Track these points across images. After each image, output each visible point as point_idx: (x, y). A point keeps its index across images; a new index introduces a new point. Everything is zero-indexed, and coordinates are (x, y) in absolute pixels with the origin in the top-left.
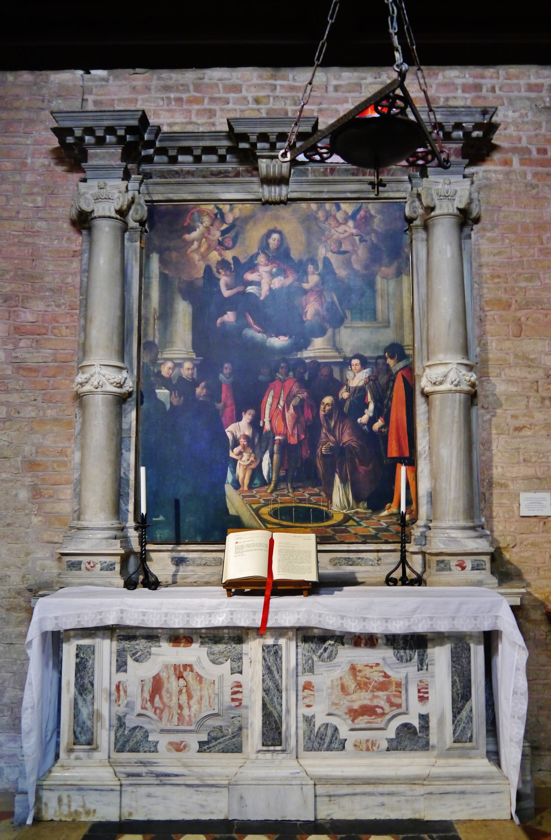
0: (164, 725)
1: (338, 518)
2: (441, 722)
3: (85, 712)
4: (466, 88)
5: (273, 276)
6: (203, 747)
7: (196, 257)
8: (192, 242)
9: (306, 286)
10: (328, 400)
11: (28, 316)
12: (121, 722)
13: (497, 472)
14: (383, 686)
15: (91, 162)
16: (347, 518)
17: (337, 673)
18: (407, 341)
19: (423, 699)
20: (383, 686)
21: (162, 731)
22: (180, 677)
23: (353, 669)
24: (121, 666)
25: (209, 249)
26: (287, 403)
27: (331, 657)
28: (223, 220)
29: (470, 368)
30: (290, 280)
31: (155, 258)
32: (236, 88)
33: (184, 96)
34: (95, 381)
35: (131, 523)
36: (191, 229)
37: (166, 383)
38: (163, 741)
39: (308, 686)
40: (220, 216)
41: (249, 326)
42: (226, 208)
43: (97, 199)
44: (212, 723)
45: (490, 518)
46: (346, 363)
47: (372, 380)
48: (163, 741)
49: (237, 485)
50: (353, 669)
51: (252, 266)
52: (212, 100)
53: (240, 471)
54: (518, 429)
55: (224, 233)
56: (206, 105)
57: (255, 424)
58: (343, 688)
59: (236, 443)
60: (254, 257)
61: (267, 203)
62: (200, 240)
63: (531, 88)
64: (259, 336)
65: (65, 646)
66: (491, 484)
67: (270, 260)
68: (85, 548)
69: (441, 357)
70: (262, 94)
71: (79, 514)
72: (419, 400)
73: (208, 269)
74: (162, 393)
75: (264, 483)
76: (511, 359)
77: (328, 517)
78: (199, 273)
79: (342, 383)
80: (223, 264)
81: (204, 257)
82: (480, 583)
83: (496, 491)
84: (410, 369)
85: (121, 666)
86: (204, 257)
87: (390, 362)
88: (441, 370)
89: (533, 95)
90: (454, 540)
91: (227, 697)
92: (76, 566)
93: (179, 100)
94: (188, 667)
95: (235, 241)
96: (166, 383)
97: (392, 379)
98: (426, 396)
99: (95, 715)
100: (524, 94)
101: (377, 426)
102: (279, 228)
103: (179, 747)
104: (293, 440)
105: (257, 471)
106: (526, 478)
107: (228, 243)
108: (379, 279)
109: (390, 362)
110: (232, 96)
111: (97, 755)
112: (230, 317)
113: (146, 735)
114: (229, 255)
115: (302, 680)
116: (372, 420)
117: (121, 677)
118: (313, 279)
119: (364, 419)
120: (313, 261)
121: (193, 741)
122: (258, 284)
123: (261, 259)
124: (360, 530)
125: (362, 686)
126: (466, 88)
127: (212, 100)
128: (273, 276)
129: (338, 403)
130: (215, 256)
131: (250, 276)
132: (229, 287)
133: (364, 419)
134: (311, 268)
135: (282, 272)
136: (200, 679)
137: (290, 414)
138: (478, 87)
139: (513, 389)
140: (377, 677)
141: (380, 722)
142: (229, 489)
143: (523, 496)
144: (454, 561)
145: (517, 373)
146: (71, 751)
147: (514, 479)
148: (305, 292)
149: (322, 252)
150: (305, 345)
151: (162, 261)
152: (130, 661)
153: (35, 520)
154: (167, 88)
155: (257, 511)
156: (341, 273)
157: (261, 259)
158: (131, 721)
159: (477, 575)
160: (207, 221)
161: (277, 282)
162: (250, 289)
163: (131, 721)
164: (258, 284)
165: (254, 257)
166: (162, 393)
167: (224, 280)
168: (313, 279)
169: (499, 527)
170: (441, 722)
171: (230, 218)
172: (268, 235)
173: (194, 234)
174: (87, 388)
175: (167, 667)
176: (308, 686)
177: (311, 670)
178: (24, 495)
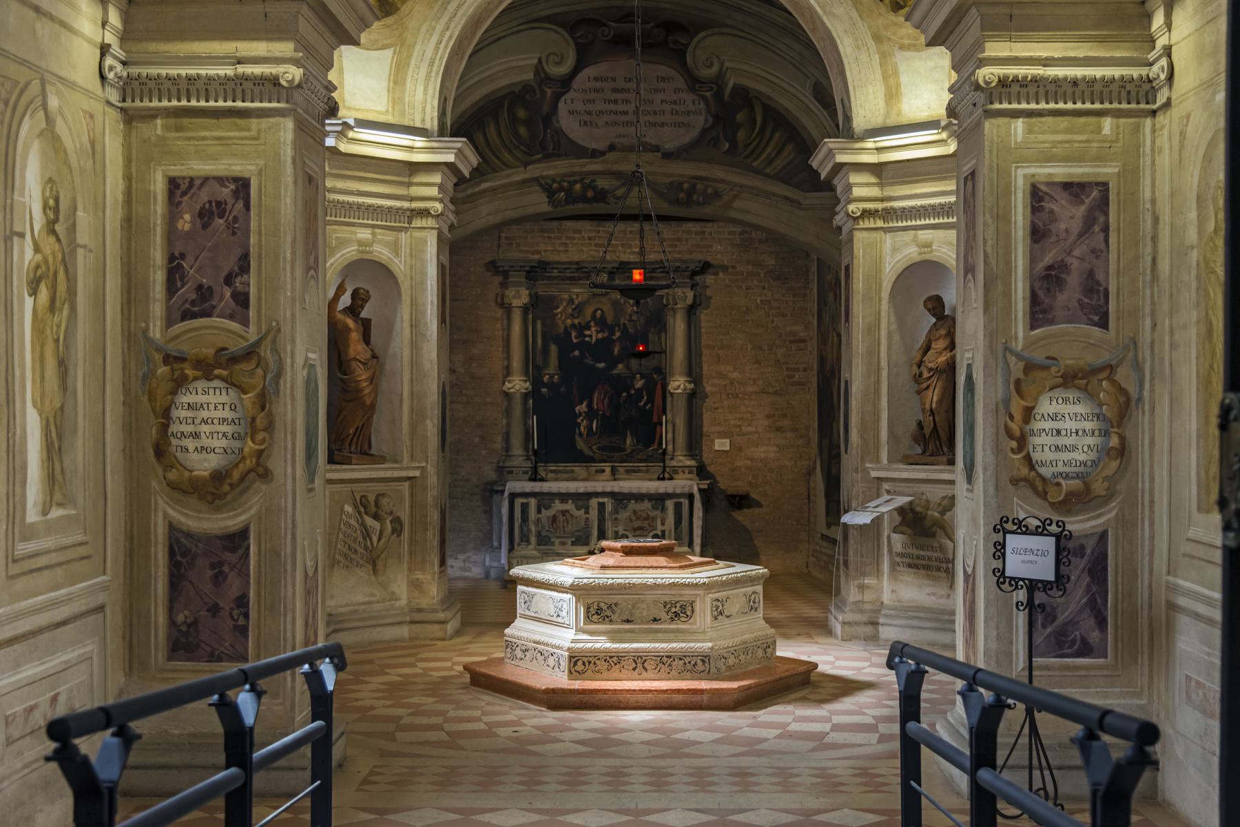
0: (558, 534)
1: (629, 451)
2: (670, 531)
3: (525, 529)
4: (697, 233)
5: (598, 332)
6: (573, 544)
7: (560, 322)
8: (557, 315)
9: (614, 338)
10: (624, 394)
11: (476, 352)
12: (539, 534)
13: (705, 429)
14: (647, 518)
15: (511, 279)
16: (633, 451)
17: (628, 514)
18: (663, 366)
19: (663, 524)
20: (647, 518)
21: (558, 537)
22: (564, 515)
23: (635, 512)
24: (539, 512)
25: (566, 319)
26: (605, 395)
27: (626, 507)
28: (573, 303)
29: (690, 382)
30: (606, 335)
31: (539, 322)
32: (579, 232)
33: (552, 235)
34: (517, 387)
35: (531, 453)
36: (558, 307)
37: (546, 385)
38: (557, 541)
39: (616, 519)
40: (571, 301)
41: (586, 357)
42: (575, 297)
43: (514, 297)
44: (577, 534)
45: (701, 451)
46: (633, 377)
47: (644, 386)
48: (557, 541)
49: (581, 435)
50: (635, 512)
51: (589, 328)
52: (567, 238)
53: (582, 429)
54: (717, 409)
55: (573, 310)
56: (563, 240)
57: (589, 406)
58: (631, 520)
59: (580, 415)
60: (590, 322)
61: (595, 295)
62: (561, 313)
63: (730, 233)
64: (591, 362)
65: (516, 500)
66: (702, 435)
67: (596, 325)
68: (515, 463)
69: (677, 377)
70: (592, 235)
71: (507, 449)
72: (668, 395)
73: (566, 328)
74: (544, 390)
75: (594, 434)
76: (714, 374)
77: (625, 450)
78: (562, 330)
79: (632, 386)
80: (573, 326)
81: (564, 322)
82: (691, 479)
83: (704, 438)
84: (664, 379)
85: (539, 512)
86: (564, 322)
87: (655, 376)
88: (677, 383)
89: (731, 237)
90: (680, 461)
91: (583, 524)
92: (511, 472)
93: (549, 238)
94: (567, 511)
95: (579, 314)
96: (546, 385)
97: (655, 384)
98: (672, 394)
99: (529, 530)
100: (726, 236)
101: (648, 407)
102: (601, 307)
103: (563, 544)
104: (608, 414)
105: (590, 428)
106: (719, 432)
107: (576, 315)
108: (650, 335)
109: (655, 376)
110: (577, 236)
111: (531, 547)
112: (577, 353)
113: (550, 538)
114: (576, 321)
115: (614, 516)
116: (646, 404)
117: (539, 516)
118: (618, 334)
119: (642, 403)
120: (619, 326)
121: (569, 541)
122: (590, 336)
123: (592, 324)
124: (639, 457)
125: (638, 518)
126: (697, 233)
127: (567, 238)
128: (598, 332)
129: (629, 396)
130: (569, 321)
131: (587, 333)
132: (576, 338)
133: (642, 403)
134: (617, 328)
135: (602, 331)
136: (572, 516)
137: (606, 401)
138: (703, 233)
139: (714, 389)
140: (644, 515)
141: (645, 533)
142: (577, 437)
143: (716, 441)
144: (680, 470)
145: (716, 381)
146: (519, 545)
147: (713, 433)
148: (614, 341)
149: (622, 322)
150: (614, 367)
151: (543, 325)
152: (543, 510)
153: (484, 452)
154: (543, 231)
155: (590, 447)
156: (631, 331)
157: (592, 324)
158: (544, 533)
159: (690, 476)
160: (565, 303)
161: (600, 336)
162: (587, 339)
163: (544, 533)
164: (590, 336)
165: (590, 322)
166: (544, 390)
167: (574, 334)
168: (618, 334)
169: (705, 456)
170: (670, 531)
171: (576, 302)
172: (597, 310)
173: (559, 310)
174: (512, 390)
175: (558, 511)
176: (616, 519)
177: (617, 513)
178: (477, 440)
